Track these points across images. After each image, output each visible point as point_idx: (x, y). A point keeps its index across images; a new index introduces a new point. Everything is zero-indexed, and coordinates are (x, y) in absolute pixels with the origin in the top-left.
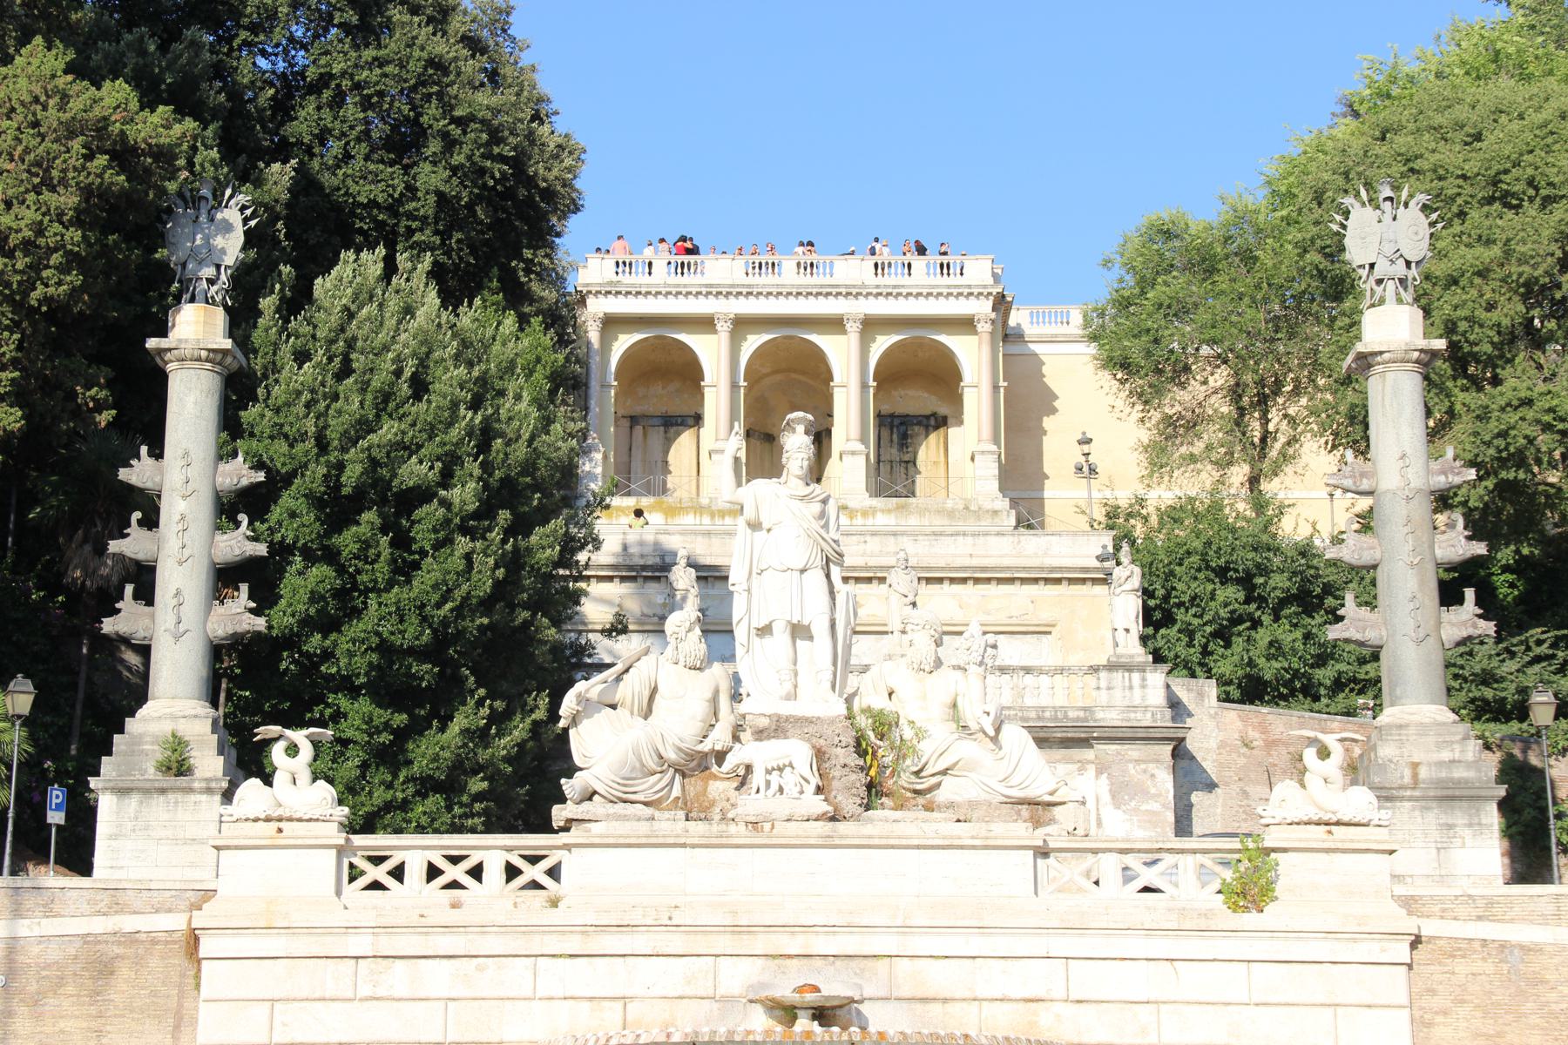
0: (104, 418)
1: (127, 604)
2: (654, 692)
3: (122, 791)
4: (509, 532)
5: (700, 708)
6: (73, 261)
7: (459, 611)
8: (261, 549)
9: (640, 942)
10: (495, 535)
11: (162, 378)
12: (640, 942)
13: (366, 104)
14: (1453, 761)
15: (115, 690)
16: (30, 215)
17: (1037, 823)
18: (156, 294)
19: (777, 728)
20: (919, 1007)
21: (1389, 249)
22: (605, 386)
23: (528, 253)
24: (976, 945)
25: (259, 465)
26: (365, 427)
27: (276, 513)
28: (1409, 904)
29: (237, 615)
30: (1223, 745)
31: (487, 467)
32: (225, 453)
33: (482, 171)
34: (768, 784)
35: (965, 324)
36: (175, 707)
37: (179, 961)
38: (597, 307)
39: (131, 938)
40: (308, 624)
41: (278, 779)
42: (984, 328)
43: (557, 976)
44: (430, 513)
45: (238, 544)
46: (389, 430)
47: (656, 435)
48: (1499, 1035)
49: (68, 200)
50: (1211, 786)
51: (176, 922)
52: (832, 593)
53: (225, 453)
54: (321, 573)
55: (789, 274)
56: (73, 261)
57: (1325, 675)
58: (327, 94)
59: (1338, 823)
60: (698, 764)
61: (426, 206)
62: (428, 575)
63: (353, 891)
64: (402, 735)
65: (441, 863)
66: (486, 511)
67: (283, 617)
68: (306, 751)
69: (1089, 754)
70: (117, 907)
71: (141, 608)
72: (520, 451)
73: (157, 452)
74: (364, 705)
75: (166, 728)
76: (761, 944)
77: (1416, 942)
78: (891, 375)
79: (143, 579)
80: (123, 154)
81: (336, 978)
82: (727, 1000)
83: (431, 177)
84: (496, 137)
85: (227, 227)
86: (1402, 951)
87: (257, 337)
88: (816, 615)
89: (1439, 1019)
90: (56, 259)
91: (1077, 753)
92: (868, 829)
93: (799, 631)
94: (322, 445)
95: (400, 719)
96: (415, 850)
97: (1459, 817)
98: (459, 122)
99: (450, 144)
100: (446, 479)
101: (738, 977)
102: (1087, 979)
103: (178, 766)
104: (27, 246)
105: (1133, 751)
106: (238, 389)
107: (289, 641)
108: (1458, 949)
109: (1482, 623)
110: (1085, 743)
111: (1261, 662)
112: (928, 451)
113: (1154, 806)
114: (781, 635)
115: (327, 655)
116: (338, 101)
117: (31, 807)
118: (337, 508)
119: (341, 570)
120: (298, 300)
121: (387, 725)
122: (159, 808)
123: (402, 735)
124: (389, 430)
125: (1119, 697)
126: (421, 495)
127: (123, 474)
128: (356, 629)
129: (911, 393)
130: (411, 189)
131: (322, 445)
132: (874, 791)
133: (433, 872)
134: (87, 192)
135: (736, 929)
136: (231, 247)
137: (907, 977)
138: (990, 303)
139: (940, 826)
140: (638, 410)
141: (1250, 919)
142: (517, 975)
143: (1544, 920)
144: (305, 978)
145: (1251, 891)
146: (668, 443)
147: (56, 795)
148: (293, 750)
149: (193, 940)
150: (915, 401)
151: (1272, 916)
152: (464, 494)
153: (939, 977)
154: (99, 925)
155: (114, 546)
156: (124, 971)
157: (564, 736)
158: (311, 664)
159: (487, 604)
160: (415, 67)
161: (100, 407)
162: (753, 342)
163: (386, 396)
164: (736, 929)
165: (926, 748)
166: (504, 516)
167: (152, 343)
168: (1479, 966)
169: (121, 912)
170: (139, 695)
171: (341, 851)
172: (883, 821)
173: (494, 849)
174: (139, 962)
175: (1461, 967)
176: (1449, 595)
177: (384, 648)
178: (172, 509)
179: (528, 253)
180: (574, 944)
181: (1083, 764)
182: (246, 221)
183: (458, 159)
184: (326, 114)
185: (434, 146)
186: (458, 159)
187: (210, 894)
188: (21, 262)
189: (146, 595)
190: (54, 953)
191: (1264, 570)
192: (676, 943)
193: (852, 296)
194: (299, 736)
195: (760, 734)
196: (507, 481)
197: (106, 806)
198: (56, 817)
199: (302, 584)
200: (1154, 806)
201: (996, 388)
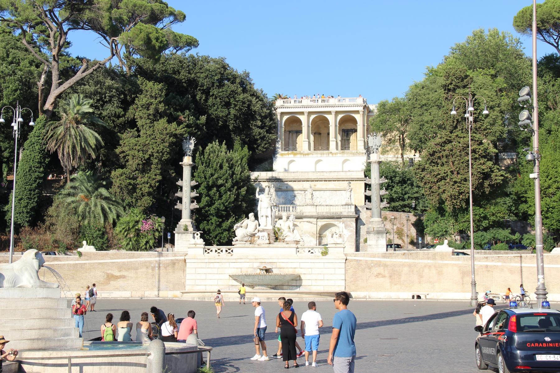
0: (174, 175)
1: (178, 203)
3: (179, 233)
4: (237, 190)
5: (254, 227)
6: (168, 153)
7: (229, 204)
8: (198, 195)
9: (243, 261)
10: (234, 191)
11: (182, 168)
12: (243, 261)
13: (220, 99)
15: (178, 216)
16: (162, 147)
17: (297, 244)
18: (181, 154)
19: (263, 231)
21: (375, 144)
22: (281, 127)
23: (251, 122)
24: (288, 261)
25: (197, 182)
26: (212, 175)
27: (200, 189)
28: (346, 255)
29: (195, 205)
30: (367, 217)
31: (233, 180)
32: (192, 180)
33: (242, 109)
35: (357, 112)
36: (186, 220)
37: (183, 263)
38: (279, 111)
39: (177, 260)
40: (206, 206)
42: (361, 113)
43: (232, 265)
44: (223, 189)
45: (194, 194)
46: (215, 177)
47: (295, 135)
49: (167, 144)
50: (364, 224)
51: (183, 258)
52: (272, 210)
53: (192, 180)
54: (207, 198)
55: (320, 103)
56: (168, 153)
57: (406, 196)
58: (214, 97)
60: (253, 235)
61: (232, 116)
62: (224, 198)
63: (206, 253)
64: (221, 223)
66: (233, 187)
67: (202, 205)
68: (199, 235)
69: (341, 220)
70: (175, 256)
71: (180, 204)
72: (238, 176)
73: (182, 180)
74: (215, 218)
75: (184, 223)
76: (259, 261)
78: (343, 121)
79: (180, 199)
80: (175, 136)
81: (203, 265)
82: (254, 268)
83: (233, 111)
84: (244, 103)
85: (191, 144)
87: (196, 161)
88: (269, 214)
90: (166, 153)
91: (339, 220)
92: (274, 245)
93: (267, 217)
94: (205, 178)
95: (221, 220)
97: (380, 236)
98: (237, 101)
99: (236, 106)
100: (226, 182)
101: (256, 265)
102: (302, 265)
103: (186, 230)
104: (161, 152)
105: (349, 219)
106: (194, 168)
107: (203, 208)
108: (352, 260)
110: (340, 218)
111: (393, 195)
112: (352, 137)
113: (352, 229)
114: (264, 217)
115: (209, 210)
116: (216, 98)
117: (165, 235)
118: (209, 188)
119: (210, 197)
120: (202, 153)
121: (218, 221)
122: (184, 236)
123: (221, 223)
124: (215, 177)
125: (346, 210)
126: (222, 185)
127: (177, 183)
128: (214, 207)
129: (349, 124)
130: (230, 113)
131: (205, 178)
132: (277, 239)
133: (216, 251)
134: (169, 143)
135: (256, 259)
136: (192, 147)
137: (279, 265)
138: (362, 108)
139: (284, 245)
140: (291, 129)
141: (324, 257)
142: (227, 265)
143: (362, 257)
145: (325, 253)
146: (297, 137)
147: (169, 234)
148: (197, 235)
149: (185, 260)
150: (349, 126)
151: (327, 256)
152: (229, 185)
153: (282, 265)
154: (173, 258)
155: (176, 195)
156: (177, 264)
157: (234, 232)
158: (206, 212)
159: (233, 202)
160: (229, 92)
161: (173, 173)
162: (313, 117)
163: (215, 170)
164: (256, 259)
165: (284, 233)
166: (236, 187)
167: (180, 163)
170: (180, 218)
171: (204, 248)
172: (277, 244)
173: (224, 248)
174: (178, 263)
175: (352, 263)
177: (218, 209)
178: (184, 189)
179: (251, 122)
180: (234, 261)
181: (340, 222)
183: (237, 108)
184: (214, 100)
185: (233, 106)
186: (237, 108)
187: (187, 254)
188: (161, 154)
189: (181, 202)
191: (395, 177)
192: (248, 261)
193: (334, 106)
194: (198, 233)
195: (261, 231)
196: (236, 181)
197: (176, 235)
198: (169, 237)
199: (205, 200)
200: (352, 229)
201: (364, 125)
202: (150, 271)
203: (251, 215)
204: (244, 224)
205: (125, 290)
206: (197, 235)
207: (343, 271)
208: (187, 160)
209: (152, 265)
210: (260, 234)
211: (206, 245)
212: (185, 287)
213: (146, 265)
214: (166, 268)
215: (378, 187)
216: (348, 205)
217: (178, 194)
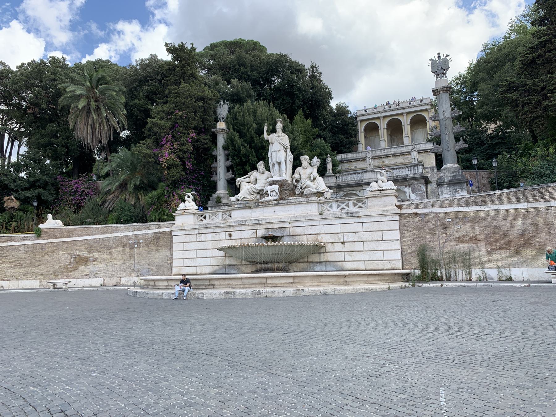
1: (214, 175)
2: (256, 180)
20: (294, 237)
39: (162, 233)
41: (186, 202)
48: (419, 234)
59: (383, 190)
68: (191, 196)
76: (264, 227)
77: (399, 216)
81: (193, 238)
86: (397, 218)
92: (285, 202)
97: (458, 187)
101: (261, 233)
102: (328, 229)
109: (464, 145)
114: (276, 166)
144: (188, 238)
148: (189, 197)
154: (157, 231)
156: (161, 238)
164: (259, 224)
174: (163, 238)
176: (457, 139)
190: (150, 236)
194: (190, 194)
202: (128, 250)
203: (261, 165)
204: (252, 179)
205: (96, 277)
206: (189, 197)
207: (397, 235)
212: (172, 269)
213: (123, 243)
214: (147, 245)
216: (415, 166)
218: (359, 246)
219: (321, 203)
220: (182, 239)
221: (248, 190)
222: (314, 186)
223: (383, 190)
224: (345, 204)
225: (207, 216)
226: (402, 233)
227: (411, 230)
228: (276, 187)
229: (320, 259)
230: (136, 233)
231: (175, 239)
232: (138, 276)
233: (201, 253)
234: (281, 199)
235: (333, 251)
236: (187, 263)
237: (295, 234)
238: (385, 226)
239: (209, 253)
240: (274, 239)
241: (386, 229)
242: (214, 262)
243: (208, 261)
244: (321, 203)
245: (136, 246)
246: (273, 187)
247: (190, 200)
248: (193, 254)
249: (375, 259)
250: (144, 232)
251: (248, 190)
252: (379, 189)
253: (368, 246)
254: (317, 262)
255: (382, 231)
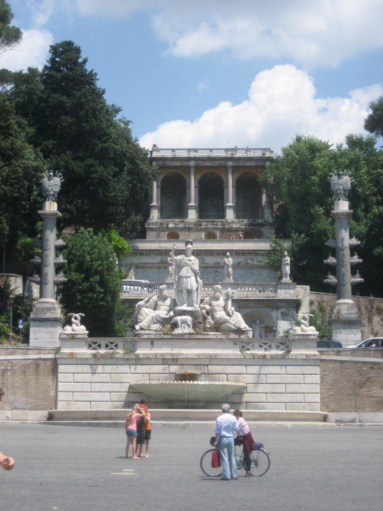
2: (156, 304)
14: (351, 313)
34: (181, 326)
41: (74, 325)
65: (109, 344)
77: (320, 361)
89: (326, 377)
93: (189, 292)
96: (103, 341)
142: (126, 368)
148: (76, 318)
154: (36, 357)
167: (39, 212)
168: (334, 365)
169: (40, 354)
182: (61, 180)
190: (27, 362)
194: (77, 315)
207: (317, 379)
208: (51, 207)
209: (2, 368)
210: (179, 318)
211: (90, 335)
215: (347, 252)
217: (37, 260)
218: (281, 388)
219: (242, 342)
220: (73, 368)
221: (153, 317)
222: (234, 323)
223: (307, 335)
224: (268, 345)
225: (103, 345)
226: (322, 378)
227: (331, 375)
228: (189, 318)
229: (241, 398)
230: (9, 357)
231: (61, 368)
232: (12, 410)
233: (96, 387)
234: (198, 334)
235: (254, 391)
236: (77, 396)
237: (214, 372)
238: (308, 369)
239: (107, 387)
240: (193, 377)
241: (307, 373)
242: (114, 396)
243: (107, 396)
244: (242, 342)
245: (9, 373)
246: (184, 317)
247: (78, 322)
248: (87, 387)
249: (295, 401)
250: (20, 357)
251: (153, 317)
252: (303, 333)
253: (291, 388)
254: (237, 403)
255: (304, 375)
